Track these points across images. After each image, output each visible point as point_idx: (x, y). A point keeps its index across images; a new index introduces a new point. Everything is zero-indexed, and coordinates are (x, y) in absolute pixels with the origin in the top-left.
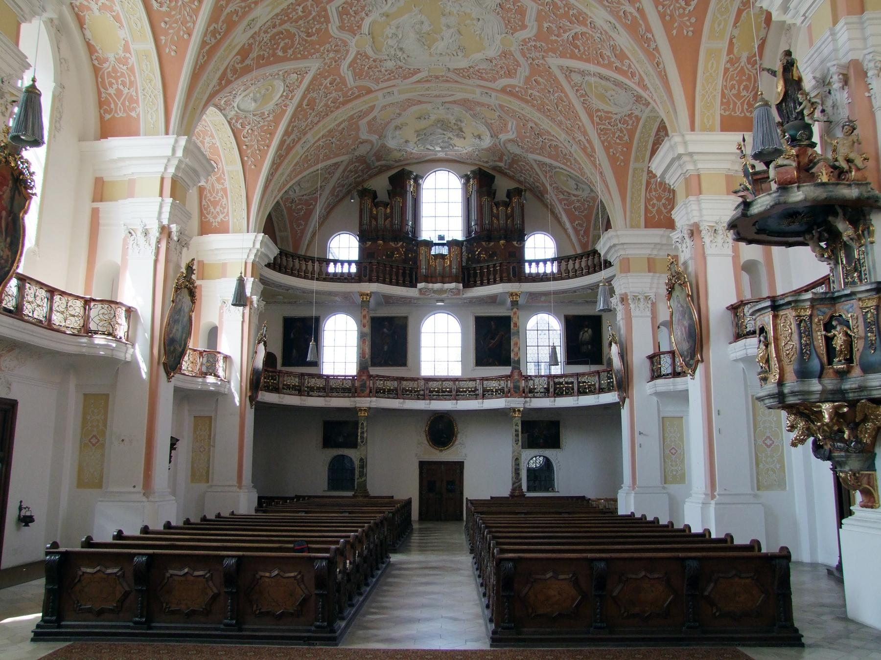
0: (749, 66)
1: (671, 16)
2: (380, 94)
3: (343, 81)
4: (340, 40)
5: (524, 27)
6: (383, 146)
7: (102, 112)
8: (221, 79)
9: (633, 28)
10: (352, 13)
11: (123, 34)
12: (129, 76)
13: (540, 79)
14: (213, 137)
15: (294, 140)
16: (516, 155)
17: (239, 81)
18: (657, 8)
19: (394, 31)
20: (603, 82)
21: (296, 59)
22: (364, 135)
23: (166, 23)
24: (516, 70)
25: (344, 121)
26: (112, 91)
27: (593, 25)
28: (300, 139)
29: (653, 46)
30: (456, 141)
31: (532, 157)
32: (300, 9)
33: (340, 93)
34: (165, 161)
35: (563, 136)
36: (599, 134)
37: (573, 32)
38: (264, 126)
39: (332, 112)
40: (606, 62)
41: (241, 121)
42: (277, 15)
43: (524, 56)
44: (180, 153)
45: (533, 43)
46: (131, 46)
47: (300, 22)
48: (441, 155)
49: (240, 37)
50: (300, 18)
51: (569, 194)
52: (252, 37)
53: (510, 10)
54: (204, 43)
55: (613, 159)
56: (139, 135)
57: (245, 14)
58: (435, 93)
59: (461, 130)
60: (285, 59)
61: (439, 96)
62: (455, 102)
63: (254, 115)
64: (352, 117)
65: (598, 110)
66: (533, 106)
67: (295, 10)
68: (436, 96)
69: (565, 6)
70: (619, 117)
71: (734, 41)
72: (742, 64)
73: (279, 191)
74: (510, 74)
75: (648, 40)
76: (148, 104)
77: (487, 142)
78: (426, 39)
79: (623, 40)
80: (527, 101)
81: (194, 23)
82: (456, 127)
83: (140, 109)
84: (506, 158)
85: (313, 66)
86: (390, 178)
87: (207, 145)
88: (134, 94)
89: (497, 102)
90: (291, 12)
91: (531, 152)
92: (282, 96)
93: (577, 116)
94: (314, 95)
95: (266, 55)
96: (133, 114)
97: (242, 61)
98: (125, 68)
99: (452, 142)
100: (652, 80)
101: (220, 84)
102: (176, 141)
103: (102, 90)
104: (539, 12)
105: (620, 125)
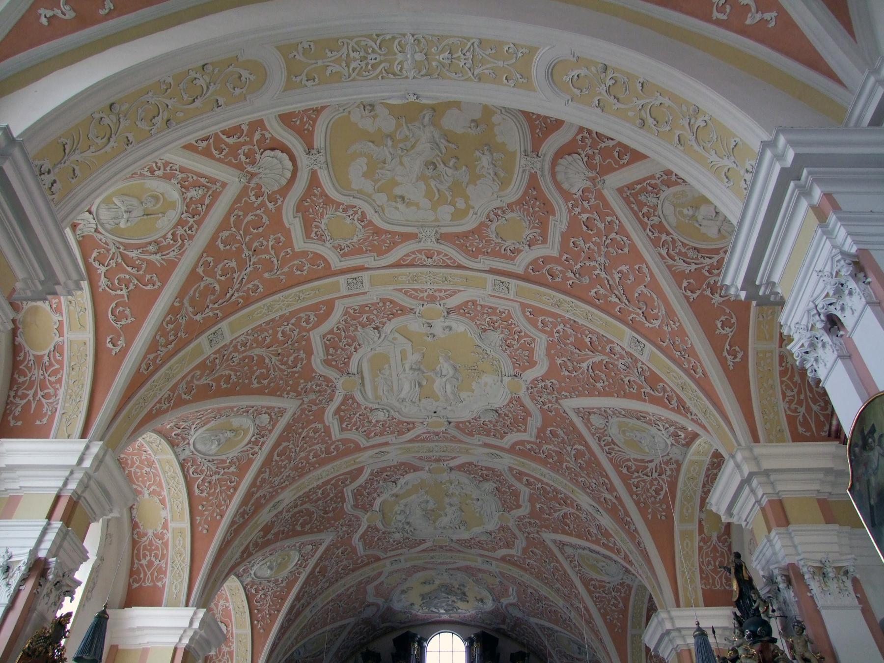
0: (721, 544)
2: (388, 562)
3: (354, 550)
4: (353, 515)
5: (519, 506)
6: (389, 609)
7: (131, 580)
8: (243, 552)
11: (163, 514)
12: (163, 550)
13: (536, 550)
14: (227, 600)
15: (303, 604)
16: (518, 619)
17: (260, 553)
19: (402, 508)
20: (594, 555)
21: (312, 532)
22: (371, 599)
23: (203, 506)
24: (514, 542)
25: (353, 586)
26: (144, 562)
27: (579, 508)
28: (309, 603)
30: (459, 604)
31: (533, 620)
32: (320, 492)
33: (350, 562)
34: (182, 632)
35: (561, 603)
36: (595, 602)
37: (563, 512)
38: (276, 592)
39: (342, 578)
40: (594, 538)
41: (255, 587)
42: (299, 497)
43: (520, 530)
44: (196, 625)
45: (528, 520)
46: (170, 525)
47: (320, 502)
48: (445, 617)
49: (265, 516)
50: (319, 499)
51: (573, 658)
52: (276, 516)
53: (505, 493)
54: (233, 522)
55: (610, 626)
56: (161, 606)
57: (272, 497)
58: (439, 561)
59: (464, 594)
60: (303, 533)
61: (443, 563)
62: (458, 569)
63: (269, 582)
64: (360, 583)
65: (592, 579)
66: (531, 573)
67: (315, 493)
68: (440, 563)
69: (553, 491)
70: (612, 585)
71: (703, 523)
72: (714, 542)
73: (284, 655)
74: (508, 545)
75: (627, 523)
76: (175, 574)
77: (489, 605)
78: (431, 515)
79: (606, 521)
80: (525, 570)
81: (227, 506)
82: (459, 592)
83: (167, 580)
84: (508, 621)
85: (328, 538)
86: (395, 641)
87: (220, 608)
88: (164, 565)
89: (498, 570)
91: (533, 616)
92: (296, 565)
93: (573, 585)
94: (327, 563)
95: (286, 530)
96: (159, 584)
97: (264, 536)
98: (160, 542)
99: (456, 605)
100: (635, 556)
101: (241, 556)
102: (195, 613)
103: (136, 561)
104: (531, 495)
105: (613, 594)
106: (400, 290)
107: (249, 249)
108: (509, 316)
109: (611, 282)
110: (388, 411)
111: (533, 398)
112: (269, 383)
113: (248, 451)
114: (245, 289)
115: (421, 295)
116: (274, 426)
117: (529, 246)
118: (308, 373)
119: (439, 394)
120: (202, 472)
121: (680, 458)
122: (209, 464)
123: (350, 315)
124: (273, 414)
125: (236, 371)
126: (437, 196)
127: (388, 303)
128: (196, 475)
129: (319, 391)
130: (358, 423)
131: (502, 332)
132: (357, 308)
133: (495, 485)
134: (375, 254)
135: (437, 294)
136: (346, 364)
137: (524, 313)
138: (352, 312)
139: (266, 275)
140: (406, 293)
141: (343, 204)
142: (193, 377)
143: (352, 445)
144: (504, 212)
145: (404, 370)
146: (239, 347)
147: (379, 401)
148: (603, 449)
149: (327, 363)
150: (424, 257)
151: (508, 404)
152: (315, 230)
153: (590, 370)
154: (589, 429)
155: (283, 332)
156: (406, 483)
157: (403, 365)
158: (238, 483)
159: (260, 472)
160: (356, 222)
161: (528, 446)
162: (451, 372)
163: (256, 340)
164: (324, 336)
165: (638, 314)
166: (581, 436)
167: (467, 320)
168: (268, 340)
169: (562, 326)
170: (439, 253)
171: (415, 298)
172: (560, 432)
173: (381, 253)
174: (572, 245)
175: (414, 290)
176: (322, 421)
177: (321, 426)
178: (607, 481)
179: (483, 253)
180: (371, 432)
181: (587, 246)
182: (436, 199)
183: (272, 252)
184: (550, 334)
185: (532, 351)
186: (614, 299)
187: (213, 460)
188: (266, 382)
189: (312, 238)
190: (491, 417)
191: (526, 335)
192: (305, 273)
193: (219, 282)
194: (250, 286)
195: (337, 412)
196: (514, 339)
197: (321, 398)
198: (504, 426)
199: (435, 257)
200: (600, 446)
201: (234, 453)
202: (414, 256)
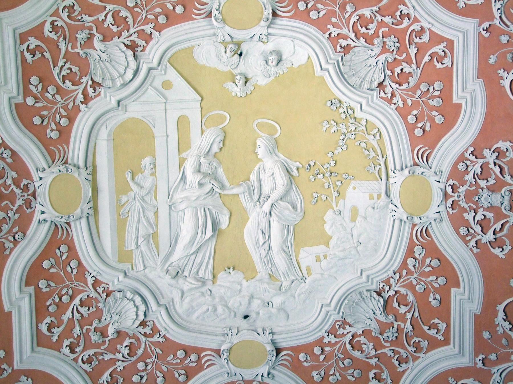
110: (145, 301)
111: (457, 222)
119: (256, 258)
130: (77, 331)
131: (385, 49)
136: (65, 134)
145: (184, 178)
147: (126, 266)
151: (404, 265)
157: (182, 162)
162: (281, 180)
164: (23, 38)
167: (312, 30)
180: (103, 366)
185: (446, 77)
191: (436, 39)
196: (408, 61)
198: (396, 341)
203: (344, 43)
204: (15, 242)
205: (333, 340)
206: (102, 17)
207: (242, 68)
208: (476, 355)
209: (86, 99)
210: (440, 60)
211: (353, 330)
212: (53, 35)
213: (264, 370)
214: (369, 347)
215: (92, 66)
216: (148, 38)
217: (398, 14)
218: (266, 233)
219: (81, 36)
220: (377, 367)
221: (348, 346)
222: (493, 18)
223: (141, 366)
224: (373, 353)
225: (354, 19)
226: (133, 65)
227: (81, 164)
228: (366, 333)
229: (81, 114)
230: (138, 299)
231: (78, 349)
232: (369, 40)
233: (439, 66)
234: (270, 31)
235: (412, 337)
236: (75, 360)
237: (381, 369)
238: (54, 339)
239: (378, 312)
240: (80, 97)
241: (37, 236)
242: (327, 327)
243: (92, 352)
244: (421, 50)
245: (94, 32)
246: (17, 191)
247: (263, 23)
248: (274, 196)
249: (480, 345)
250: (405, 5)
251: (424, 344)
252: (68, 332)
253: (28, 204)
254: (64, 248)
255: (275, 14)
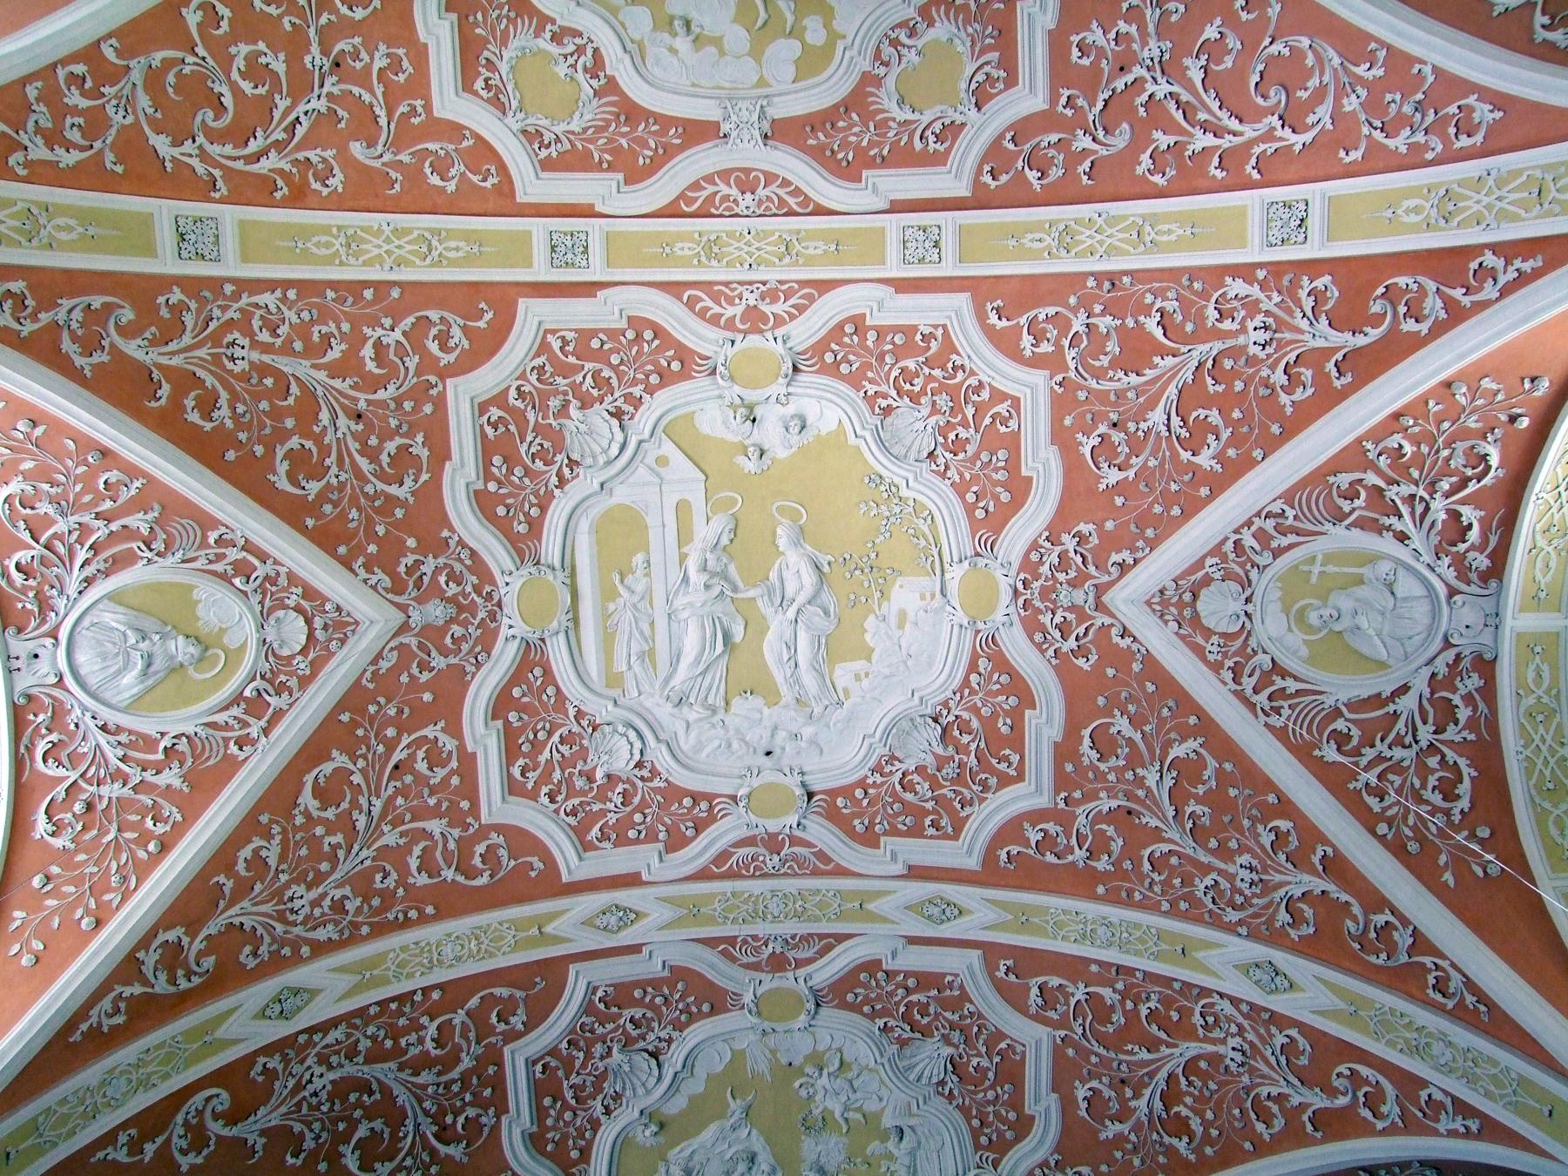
1: (1421, 840)
9: (1327, 940)
10: (569, 1094)
18: (1373, 833)
23: (48, 878)
29: (1403, 939)
32: (432, 1030)
47: (425, 1077)
79: (1313, 994)
90: (406, 1031)
95: (309, 1144)
106: (673, 288)
107: (325, 52)
108: (949, 347)
109: (1185, 97)
111: (1032, 626)
112: (322, 497)
113: (227, 727)
114: (300, 156)
115: (730, 311)
116: (316, 666)
117: (978, 106)
118: (428, 517)
119: (779, 679)
120: (74, 760)
121: (1486, 638)
122: (102, 739)
123: (553, 359)
124: (318, 622)
125: (235, 398)
126: (763, 15)
127: (648, 335)
128: (52, 770)
129: (452, 600)
130: (557, 775)
131: (935, 410)
132: (570, 336)
133: (948, 1051)
134: (620, 176)
135: (767, 308)
136: (535, 527)
137: (981, 317)
138: (556, 345)
139: (357, 149)
140: (691, 304)
141: (553, 22)
142: (108, 308)
143: (538, 865)
144: (912, 33)
145: (686, 579)
146: (256, 323)
147: (616, 693)
148: (1252, 707)
149: (483, 503)
150: (734, 192)
151: (966, 682)
152: (485, 73)
153: (1176, 421)
154: (1199, 652)
155: (378, 345)
156: (689, 1063)
157: (683, 558)
158: (179, 830)
159: (248, 826)
160: (580, 76)
161: (1034, 836)
162: (809, 578)
163: (302, 331)
164: (483, 408)
165: (1269, 136)
166: (1185, 703)
167: (843, 387)
168: (334, 354)
169: (1082, 316)
170: (770, 178)
171: (715, 321)
172: (1121, 724)
173: (635, 176)
174: (1075, 52)
175: (706, 286)
176: (455, 730)
177: (449, 744)
178: (1284, 825)
179: (871, 164)
180: (593, 817)
181: (1112, 35)
182: (759, 23)
183: (379, 90)
184: (1052, 363)
186: (1203, 141)
187: (119, 730)
188: (314, 487)
189: (476, 94)
190: (922, 747)
191: (998, 396)
192: (451, 187)
193: (236, 91)
194: (313, 155)
195: (501, 705)
196: (965, 425)
197: (457, 630)
198: (958, 779)
199: (762, 192)
200: (1239, 695)
201: (181, 721)
202: (711, 189)
203: (884, 403)
204: (478, 665)
205: (879, 779)
206: (579, 378)
207: (757, 437)
208: (1057, 793)
209: (562, 481)
210: (1004, 423)
211: (904, 767)
212: (519, 404)
213: (793, 819)
214: (923, 787)
215: (568, 441)
216: (637, 403)
217: (950, 365)
218: (792, 647)
219: (554, 403)
220: (935, 811)
221: (898, 787)
222: (1067, 369)
223: (638, 818)
224: (929, 794)
225: (895, 373)
226: (619, 437)
227: (557, 564)
228: (920, 770)
229: (555, 502)
230: (632, 735)
231: (559, 798)
232: (915, 399)
233: (1003, 429)
234: (791, 390)
235: (977, 773)
236: (557, 811)
237: (939, 813)
238: (530, 786)
239: (934, 744)
240: (554, 480)
241: (505, 656)
242: (871, 763)
243: (576, 801)
244: (979, 410)
245: (570, 397)
246: (479, 600)
247: (781, 380)
248: (801, 599)
249: (1061, 781)
250: (958, 354)
251: (993, 781)
252: (546, 777)
253: (492, 616)
254: (538, 671)
255: (795, 369)
